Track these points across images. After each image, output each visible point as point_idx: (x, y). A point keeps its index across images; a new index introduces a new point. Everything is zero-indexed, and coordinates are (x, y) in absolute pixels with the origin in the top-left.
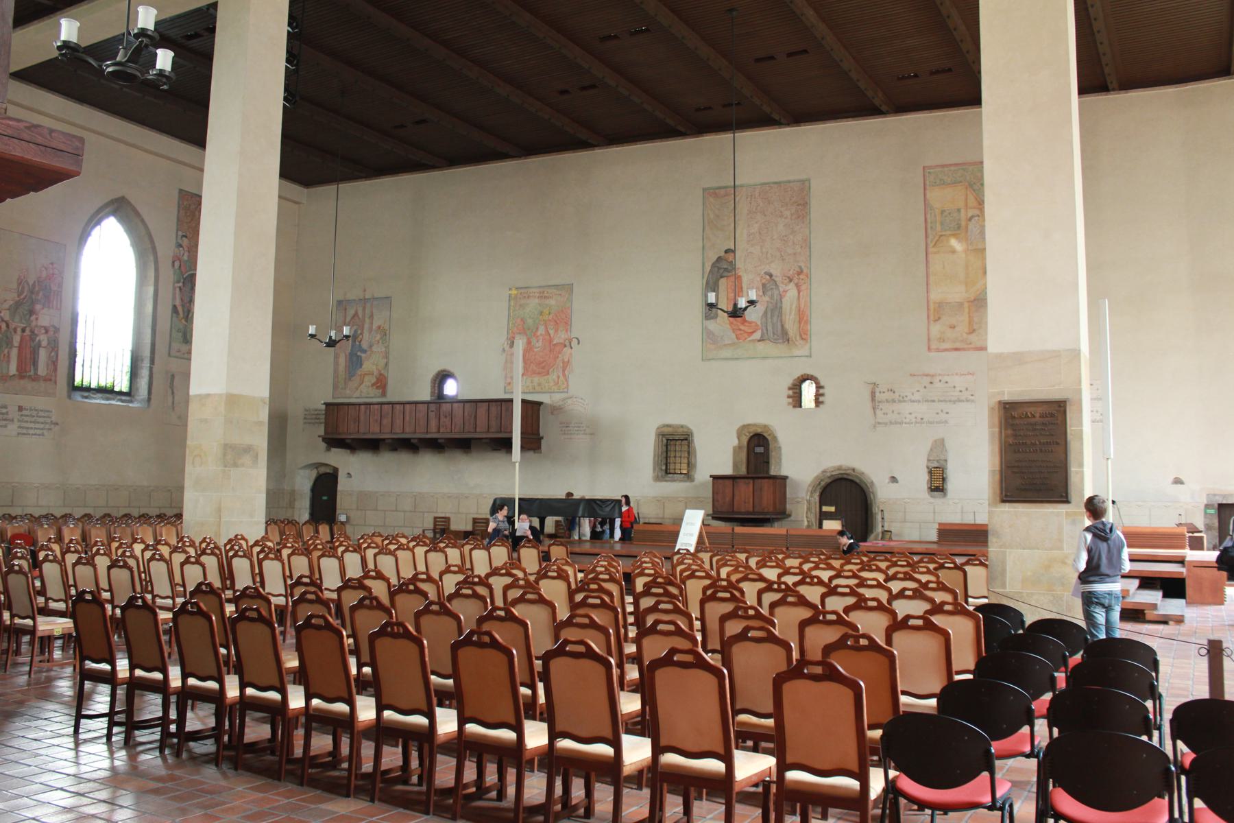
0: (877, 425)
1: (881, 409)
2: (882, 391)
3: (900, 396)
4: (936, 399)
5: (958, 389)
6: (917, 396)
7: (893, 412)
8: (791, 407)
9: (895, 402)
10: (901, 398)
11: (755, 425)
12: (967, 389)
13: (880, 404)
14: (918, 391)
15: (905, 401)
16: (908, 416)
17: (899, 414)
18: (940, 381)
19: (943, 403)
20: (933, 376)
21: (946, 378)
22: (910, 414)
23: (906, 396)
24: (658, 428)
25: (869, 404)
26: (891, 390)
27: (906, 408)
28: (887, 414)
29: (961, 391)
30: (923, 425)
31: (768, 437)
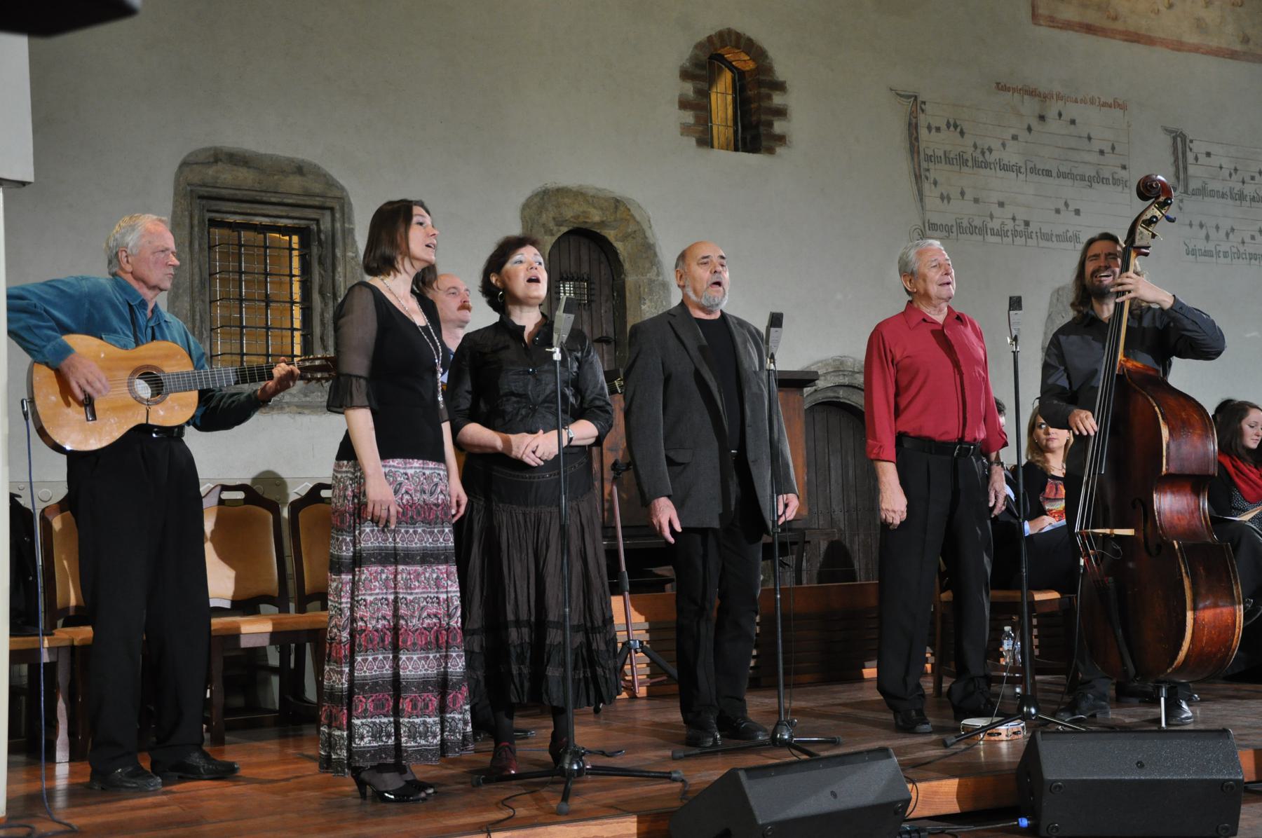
0: (928, 233)
1: (935, 183)
2: (934, 125)
3: (975, 146)
4: (1051, 165)
5: (1097, 145)
6: (1012, 155)
7: (963, 194)
8: (693, 141)
9: (965, 163)
10: (978, 154)
11: (578, 194)
12: (1113, 148)
13: (931, 166)
14: (1015, 138)
15: (987, 165)
16: (997, 211)
17: (976, 201)
18: (1060, 115)
19: (1069, 182)
20: (1044, 97)
21: (1072, 110)
22: (1001, 204)
23: (990, 150)
24: (185, 164)
25: (903, 165)
26: (956, 126)
27: (997, 185)
28: (949, 199)
29: (1102, 152)
30: (1029, 241)
31: (619, 246)
